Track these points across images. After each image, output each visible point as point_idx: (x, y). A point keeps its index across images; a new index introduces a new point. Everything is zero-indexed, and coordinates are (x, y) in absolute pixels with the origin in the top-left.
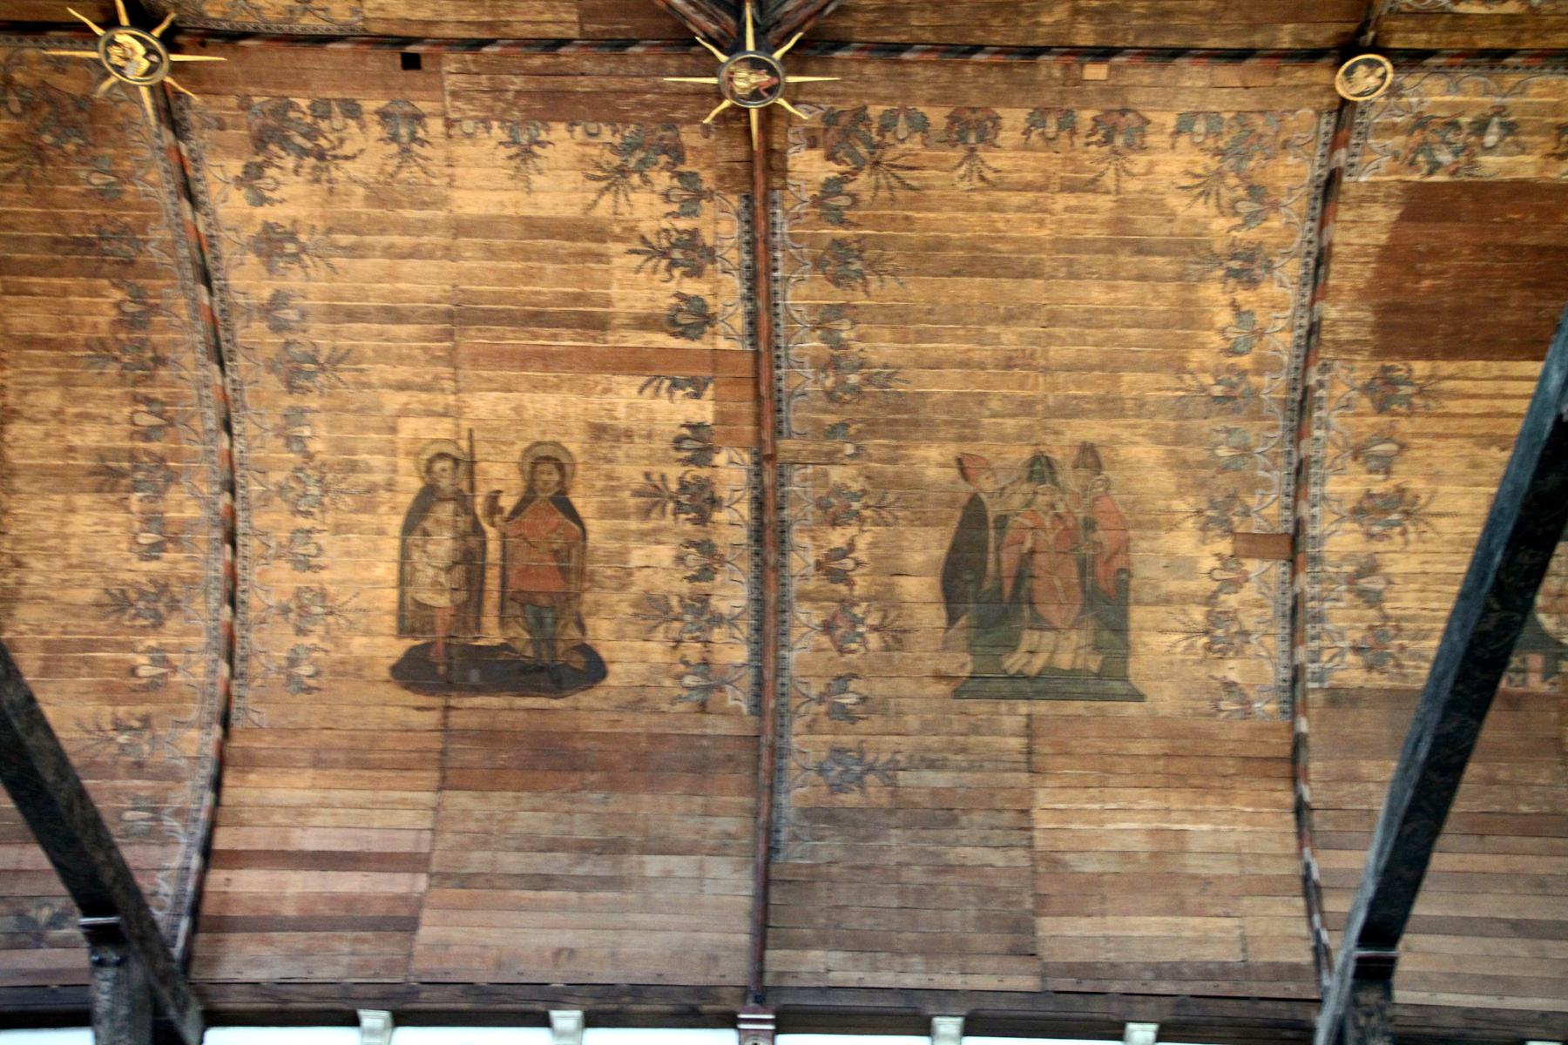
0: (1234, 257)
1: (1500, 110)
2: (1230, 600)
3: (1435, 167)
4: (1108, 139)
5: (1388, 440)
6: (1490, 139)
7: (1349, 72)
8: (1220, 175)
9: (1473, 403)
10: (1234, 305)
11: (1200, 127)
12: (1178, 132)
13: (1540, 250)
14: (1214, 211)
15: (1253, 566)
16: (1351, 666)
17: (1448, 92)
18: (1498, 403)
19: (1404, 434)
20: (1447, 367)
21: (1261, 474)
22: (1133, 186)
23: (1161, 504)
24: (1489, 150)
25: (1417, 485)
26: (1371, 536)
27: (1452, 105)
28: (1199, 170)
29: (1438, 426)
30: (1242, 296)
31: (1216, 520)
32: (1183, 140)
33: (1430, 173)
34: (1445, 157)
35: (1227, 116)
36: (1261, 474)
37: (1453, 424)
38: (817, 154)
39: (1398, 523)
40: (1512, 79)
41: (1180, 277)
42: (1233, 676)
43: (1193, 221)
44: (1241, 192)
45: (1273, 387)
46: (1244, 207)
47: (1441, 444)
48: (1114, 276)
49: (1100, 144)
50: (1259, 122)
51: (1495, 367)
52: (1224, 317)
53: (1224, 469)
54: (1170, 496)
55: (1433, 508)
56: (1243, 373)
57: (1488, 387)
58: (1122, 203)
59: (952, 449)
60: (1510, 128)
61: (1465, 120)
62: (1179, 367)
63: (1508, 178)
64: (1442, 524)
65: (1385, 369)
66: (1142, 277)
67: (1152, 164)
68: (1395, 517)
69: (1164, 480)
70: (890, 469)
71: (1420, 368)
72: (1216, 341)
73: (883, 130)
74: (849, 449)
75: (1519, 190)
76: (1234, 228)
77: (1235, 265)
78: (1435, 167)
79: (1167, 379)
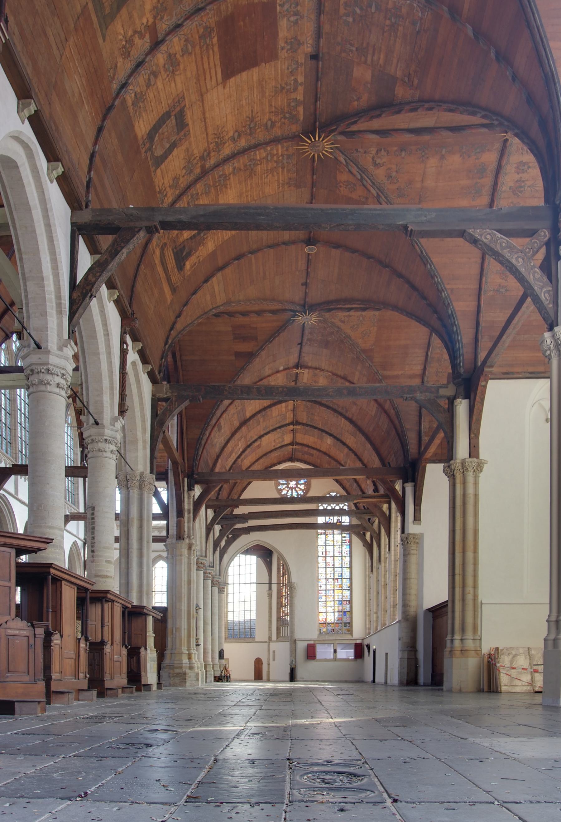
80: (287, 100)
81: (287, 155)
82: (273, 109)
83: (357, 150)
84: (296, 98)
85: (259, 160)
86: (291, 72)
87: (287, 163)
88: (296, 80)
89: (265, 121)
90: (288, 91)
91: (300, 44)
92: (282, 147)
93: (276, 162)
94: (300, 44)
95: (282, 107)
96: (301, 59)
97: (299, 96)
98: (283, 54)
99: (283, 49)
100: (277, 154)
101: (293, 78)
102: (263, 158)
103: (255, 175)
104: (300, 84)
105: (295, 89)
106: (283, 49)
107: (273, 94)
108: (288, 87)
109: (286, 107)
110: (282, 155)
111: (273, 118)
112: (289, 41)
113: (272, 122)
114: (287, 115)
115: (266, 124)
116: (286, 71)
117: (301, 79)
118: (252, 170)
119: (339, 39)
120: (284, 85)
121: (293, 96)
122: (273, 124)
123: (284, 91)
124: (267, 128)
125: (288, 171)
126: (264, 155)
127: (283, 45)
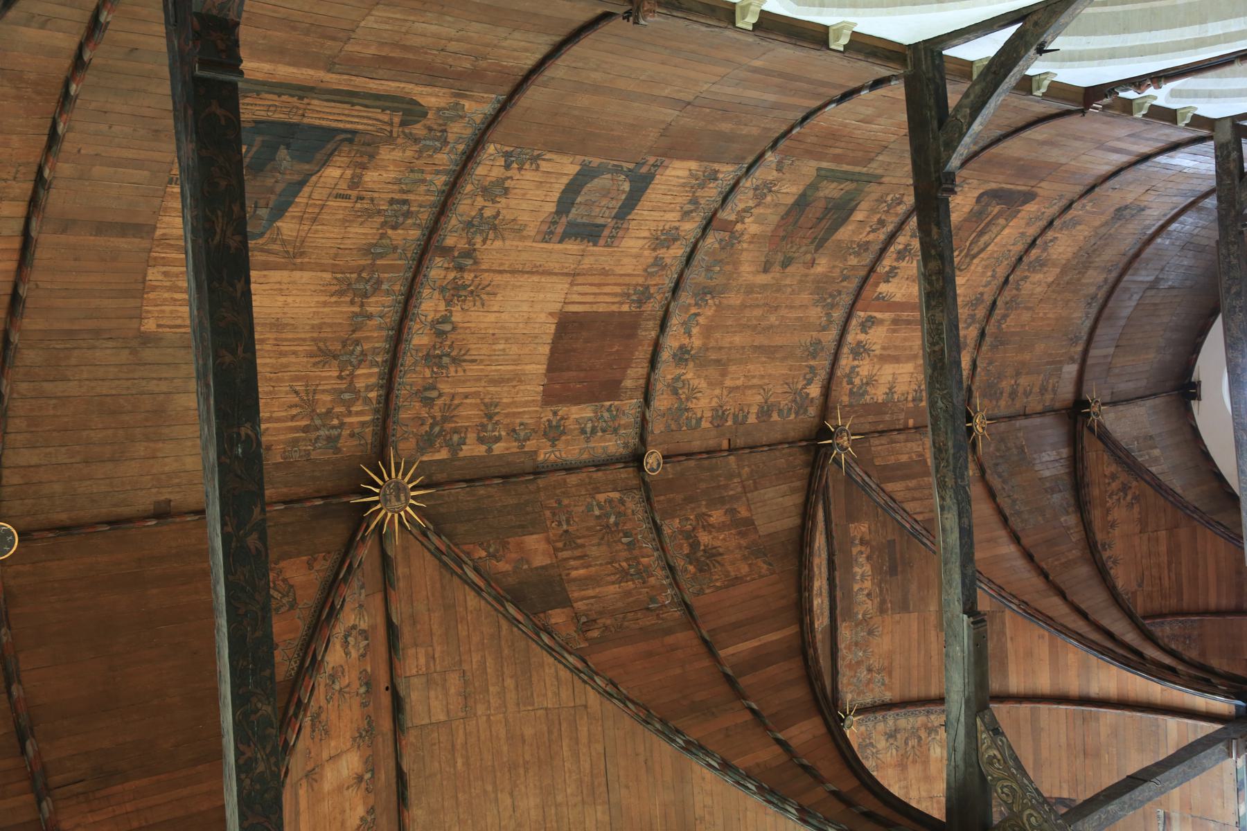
0: (686, 360)
1: (588, 440)
2: (751, 204)
3: (609, 410)
4: (723, 413)
5: (649, 273)
6: (589, 425)
7: (659, 465)
8: (687, 399)
9: (609, 291)
10: (690, 336)
11: (694, 421)
12: (701, 418)
13: (569, 369)
14: (691, 382)
15: (733, 217)
16: (722, 172)
17: (607, 447)
18: (598, 291)
19: (643, 276)
20: (615, 308)
21: (706, 258)
22: (717, 392)
23: (752, 246)
24: (590, 419)
25: (646, 253)
26: (677, 229)
27: (605, 441)
28: (694, 401)
29: (627, 280)
30: (686, 341)
31: (735, 237)
32: (699, 416)
33: (611, 406)
34: (606, 415)
35: (684, 428)
36: (706, 258)
37: (621, 281)
38: (812, 396)
39: (662, 234)
40: (585, 456)
41: (707, 349)
42: (775, 173)
43: (699, 377)
44: (680, 391)
45: (685, 298)
46: (680, 384)
47: (630, 271)
48: (730, 349)
49: (726, 410)
50: (673, 427)
51: (595, 308)
52: (695, 331)
53: (721, 261)
54: (746, 250)
55: (646, 241)
56: (696, 304)
57: (600, 299)
58: (721, 383)
59: (812, 271)
60: (583, 431)
61: (600, 434)
62: (719, 307)
63: (582, 406)
64: (646, 234)
65: (640, 307)
66: (720, 348)
67: (710, 403)
68: (663, 237)
69: (745, 256)
70: (837, 263)
71: (625, 308)
72: (701, 320)
73: (790, 409)
74: (845, 272)
75: (576, 400)
76: (684, 374)
77: (687, 356)
78: (609, 410)
79: (725, 302)
80: (467, 428)
81: (340, 435)
82: (456, 402)
83: (362, 587)
84: (464, 444)
85: (352, 375)
86: (514, 430)
87: (317, 438)
88: (498, 439)
89: (440, 386)
90: (483, 426)
91: (554, 441)
92: (363, 424)
93: (329, 412)
94: (554, 441)
95: (454, 419)
96: (530, 445)
97: (472, 449)
98: (547, 415)
99: (555, 413)
100: (350, 413)
101: (503, 433)
102: (351, 382)
103: (315, 364)
104: (490, 448)
105: (481, 440)
106: (555, 413)
107: (486, 400)
108: (490, 427)
109: (453, 425)
110: (342, 425)
111: (439, 402)
112: (562, 422)
113: (433, 399)
114: (437, 429)
115: (434, 388)
116: (518, 421)
117: (498, 448)
118: (335, 357)
119: (566, 502)
120: (496, 418)
121: (471, 437)
122: (428, 402)
123: (485, 420)
124: (426, 389)
125: (295, 441)
126: (360, 384)
127: (560, 413)
